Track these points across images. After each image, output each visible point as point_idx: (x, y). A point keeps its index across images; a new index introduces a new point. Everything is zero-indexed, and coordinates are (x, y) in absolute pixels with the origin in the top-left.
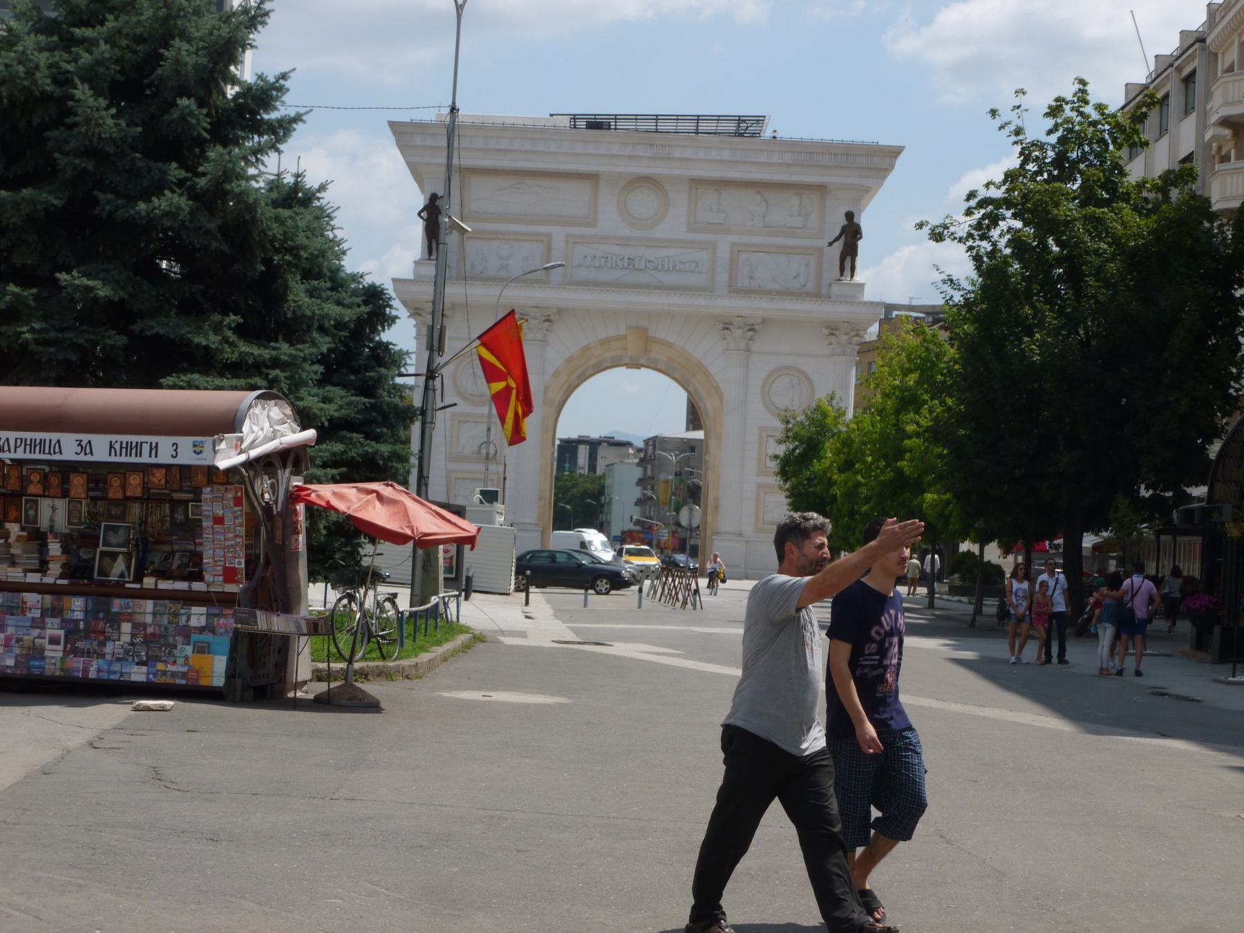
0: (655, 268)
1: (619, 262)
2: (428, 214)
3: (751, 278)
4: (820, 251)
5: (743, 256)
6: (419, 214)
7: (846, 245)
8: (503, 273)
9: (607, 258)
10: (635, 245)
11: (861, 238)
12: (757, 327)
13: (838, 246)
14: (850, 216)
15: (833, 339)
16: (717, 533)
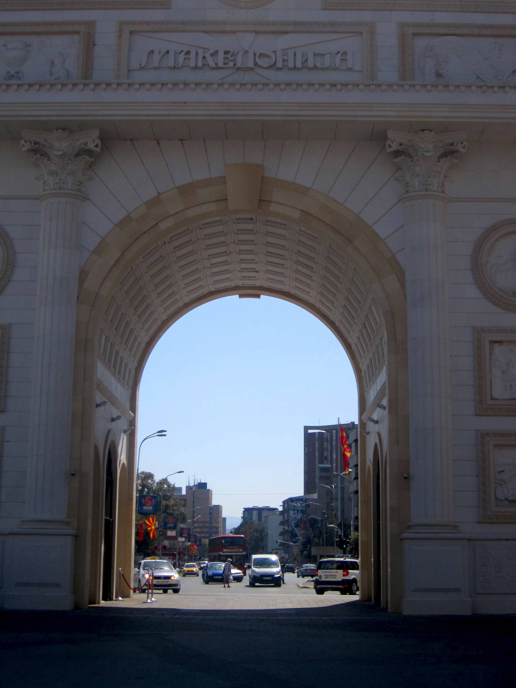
5: (421, 43)
9: (188, 53)
10: (234, 32)
12: (460, 148)
16: (409, 527)
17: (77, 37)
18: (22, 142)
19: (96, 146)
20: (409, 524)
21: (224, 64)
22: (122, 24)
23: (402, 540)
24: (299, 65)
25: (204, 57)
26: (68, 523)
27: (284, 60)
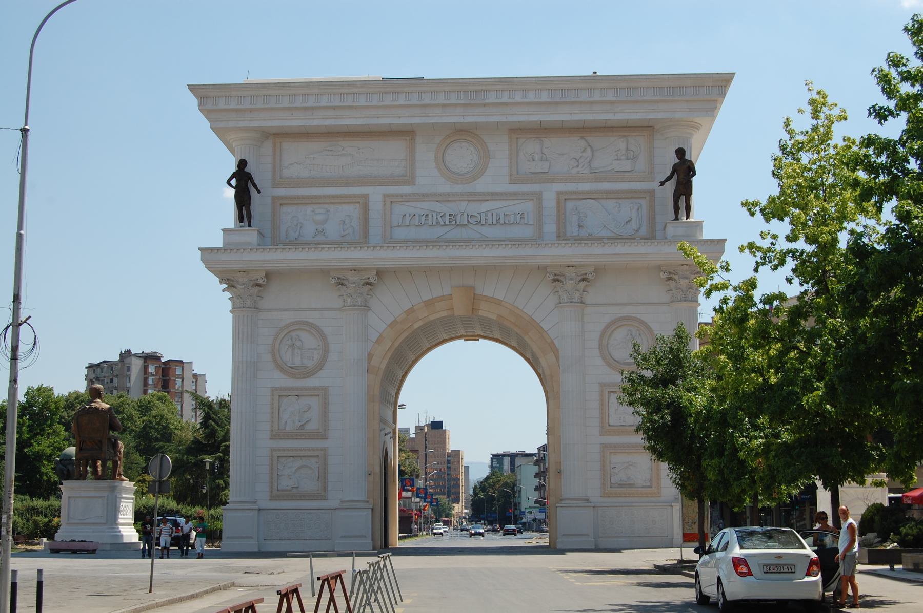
0: (479, 223)
1: (439, 217)
2: (237, 181)
3: (580, 226)
4: (651, 193)
5: (570, 205)
6: (229, 183)
7: (678, 183)
8: (320, 238)
9: (427, 215)
10: (455, 201)
11: (694, 174)
12: (590, 277)
13: (671, 186)
14: (680, 153)
15: (672, 284)
16: (561, 500)
17: (358, 205)
18: (331, 278)
19: (375, 280)
20: (561, 498)
21: (449, 222)
22: (385, 196)
23: (557, 507)
24: (495, 222)
25: (437, 218)
26: (368, 502)
27: (485, 219)
